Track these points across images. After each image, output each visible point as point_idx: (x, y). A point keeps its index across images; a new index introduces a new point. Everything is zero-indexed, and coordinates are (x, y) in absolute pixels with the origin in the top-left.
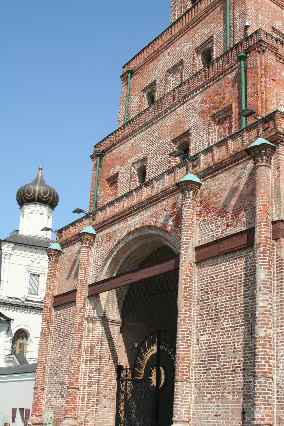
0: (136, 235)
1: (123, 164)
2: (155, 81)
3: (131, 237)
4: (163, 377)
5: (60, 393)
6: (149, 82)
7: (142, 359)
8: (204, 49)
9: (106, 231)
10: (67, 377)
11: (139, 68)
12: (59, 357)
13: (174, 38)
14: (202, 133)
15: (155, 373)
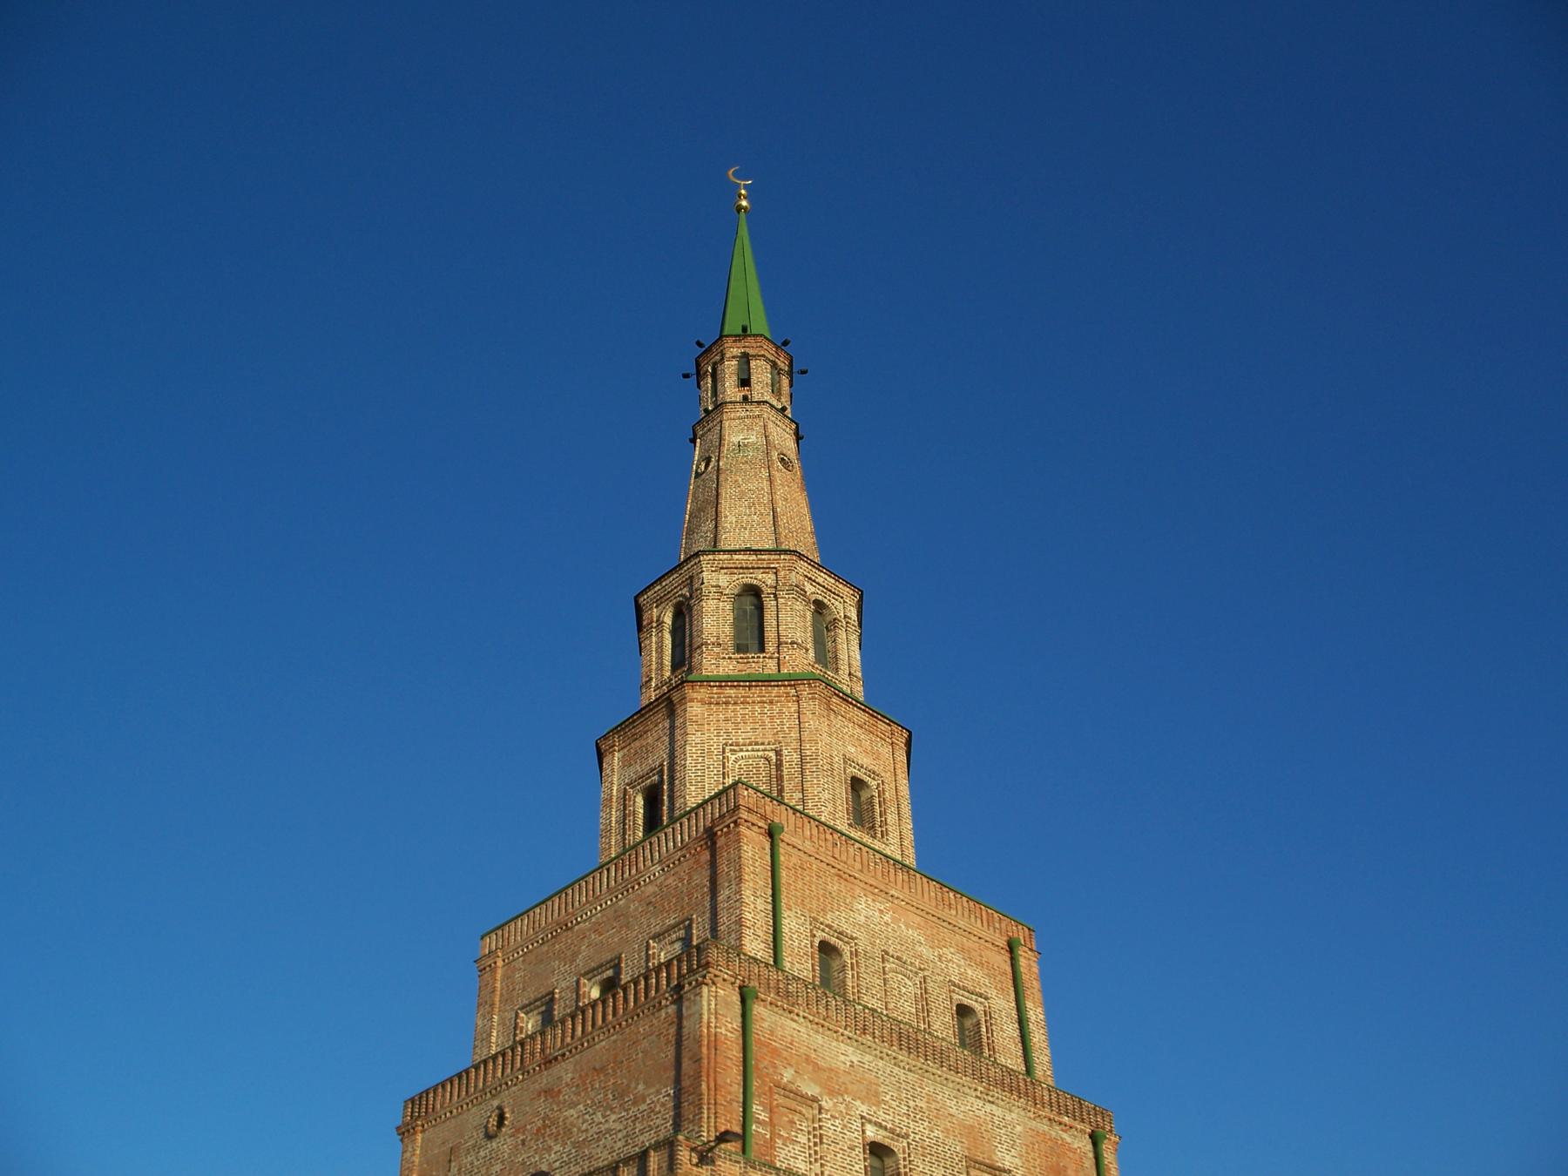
1: (832, 1093)
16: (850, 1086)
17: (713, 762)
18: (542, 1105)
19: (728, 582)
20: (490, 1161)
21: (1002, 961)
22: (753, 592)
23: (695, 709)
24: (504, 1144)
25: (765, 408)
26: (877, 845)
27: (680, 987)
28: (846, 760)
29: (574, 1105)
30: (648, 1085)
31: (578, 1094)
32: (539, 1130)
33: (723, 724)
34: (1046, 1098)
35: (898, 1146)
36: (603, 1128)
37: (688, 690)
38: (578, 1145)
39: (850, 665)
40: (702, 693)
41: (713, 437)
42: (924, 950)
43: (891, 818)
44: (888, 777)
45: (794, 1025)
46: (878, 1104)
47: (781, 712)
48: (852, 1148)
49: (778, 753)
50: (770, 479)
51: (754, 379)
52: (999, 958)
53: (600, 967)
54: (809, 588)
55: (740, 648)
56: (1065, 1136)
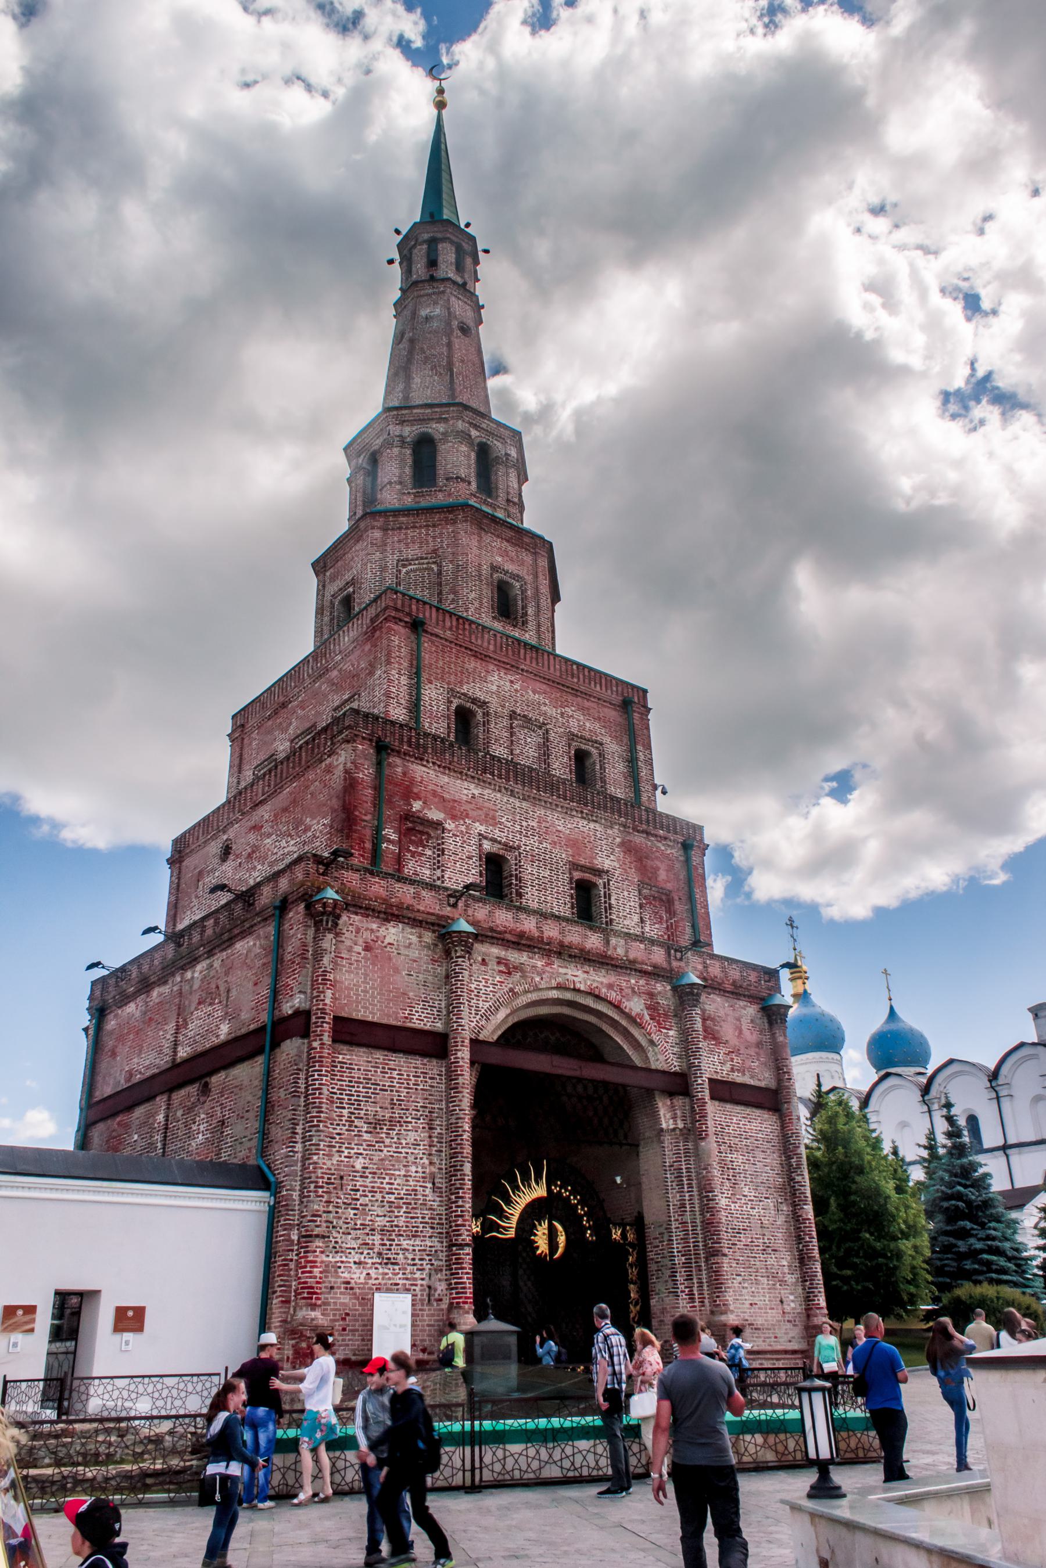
0: (568, 996)
1: (454, 818)
2: (485, 703)
3: (554, 994)
4: (562, 1239)
5: (380, 1254)
6: (465, 689)
7: (509, 1202)
8: (583, 747)
9: (495, 951)
10: (403, 1219)
11: (437, 636)
12: (358, 1167)
13: (523, 667)
14: (626, 893)
15: (546, 1232)
16: (470, 813)
18: (252, 837)
25: (448, 284)
26: (516, 634)
29: (269, 835)
31: (272, 827)
32: (249, 854)
33: (397, 545)
34: (644, 817)
36: (286, 850)
39: (508, 493)
42: (551, 711)
43: (530, 611)
44: (529, 578)
45: (424, 769)
46: (494, 825)
47: (441, 534)
48: (470, 858)
49: (440, 566)
50: (449, 345)
52: (613, 713)
54: (474, 433)
56: (659, 845)
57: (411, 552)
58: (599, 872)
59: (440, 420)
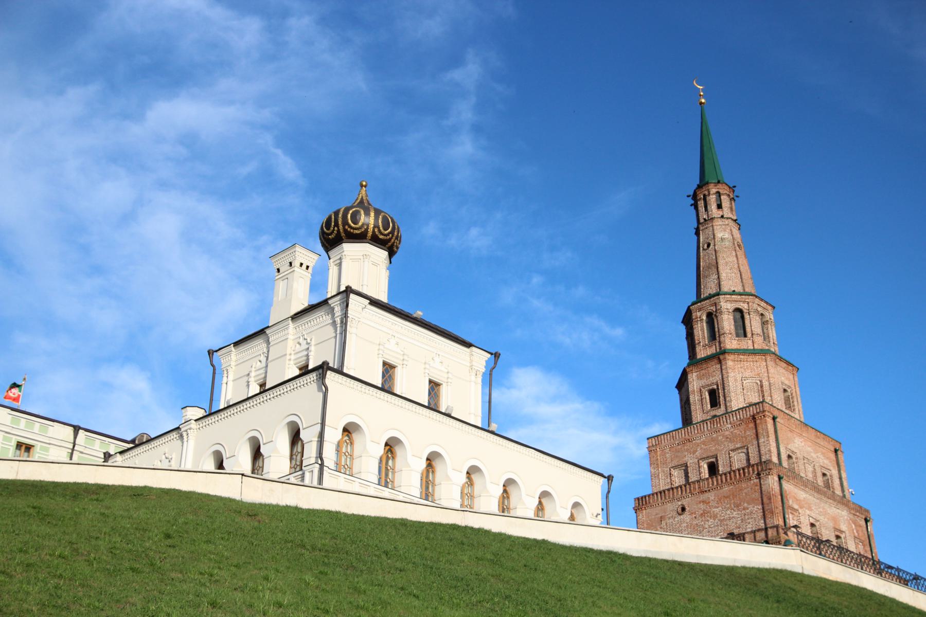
1: (801, 508)
17: (739, 383)
18: (702, 506)
19: (730, 306)
20: (681, 523)
21: (833, 456)
22: (739, 311)
23: (730, 363)
24: (686, 517)
27: (759, 474)
28: (782, 383)
30: (749, 504)
35: (817, 524)
37: (727, 356)
38: (721, 521)
40: (731, 357)
41: (709, 232)
42: (812, 454)
43: (796, 403)
44: (793, 387)
49: (761, 381)
51: (723, 205)
53: (708, 457)
55: (737, 335)
57: (748, 374)
58: (842, 532)
59: (744, 302)
